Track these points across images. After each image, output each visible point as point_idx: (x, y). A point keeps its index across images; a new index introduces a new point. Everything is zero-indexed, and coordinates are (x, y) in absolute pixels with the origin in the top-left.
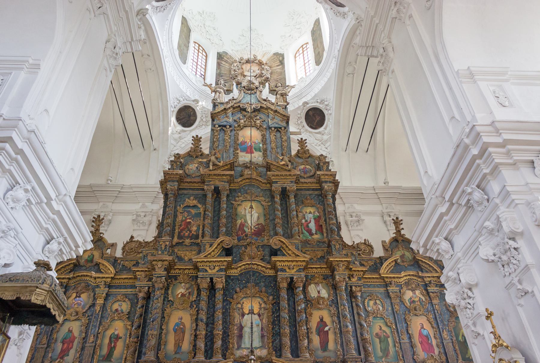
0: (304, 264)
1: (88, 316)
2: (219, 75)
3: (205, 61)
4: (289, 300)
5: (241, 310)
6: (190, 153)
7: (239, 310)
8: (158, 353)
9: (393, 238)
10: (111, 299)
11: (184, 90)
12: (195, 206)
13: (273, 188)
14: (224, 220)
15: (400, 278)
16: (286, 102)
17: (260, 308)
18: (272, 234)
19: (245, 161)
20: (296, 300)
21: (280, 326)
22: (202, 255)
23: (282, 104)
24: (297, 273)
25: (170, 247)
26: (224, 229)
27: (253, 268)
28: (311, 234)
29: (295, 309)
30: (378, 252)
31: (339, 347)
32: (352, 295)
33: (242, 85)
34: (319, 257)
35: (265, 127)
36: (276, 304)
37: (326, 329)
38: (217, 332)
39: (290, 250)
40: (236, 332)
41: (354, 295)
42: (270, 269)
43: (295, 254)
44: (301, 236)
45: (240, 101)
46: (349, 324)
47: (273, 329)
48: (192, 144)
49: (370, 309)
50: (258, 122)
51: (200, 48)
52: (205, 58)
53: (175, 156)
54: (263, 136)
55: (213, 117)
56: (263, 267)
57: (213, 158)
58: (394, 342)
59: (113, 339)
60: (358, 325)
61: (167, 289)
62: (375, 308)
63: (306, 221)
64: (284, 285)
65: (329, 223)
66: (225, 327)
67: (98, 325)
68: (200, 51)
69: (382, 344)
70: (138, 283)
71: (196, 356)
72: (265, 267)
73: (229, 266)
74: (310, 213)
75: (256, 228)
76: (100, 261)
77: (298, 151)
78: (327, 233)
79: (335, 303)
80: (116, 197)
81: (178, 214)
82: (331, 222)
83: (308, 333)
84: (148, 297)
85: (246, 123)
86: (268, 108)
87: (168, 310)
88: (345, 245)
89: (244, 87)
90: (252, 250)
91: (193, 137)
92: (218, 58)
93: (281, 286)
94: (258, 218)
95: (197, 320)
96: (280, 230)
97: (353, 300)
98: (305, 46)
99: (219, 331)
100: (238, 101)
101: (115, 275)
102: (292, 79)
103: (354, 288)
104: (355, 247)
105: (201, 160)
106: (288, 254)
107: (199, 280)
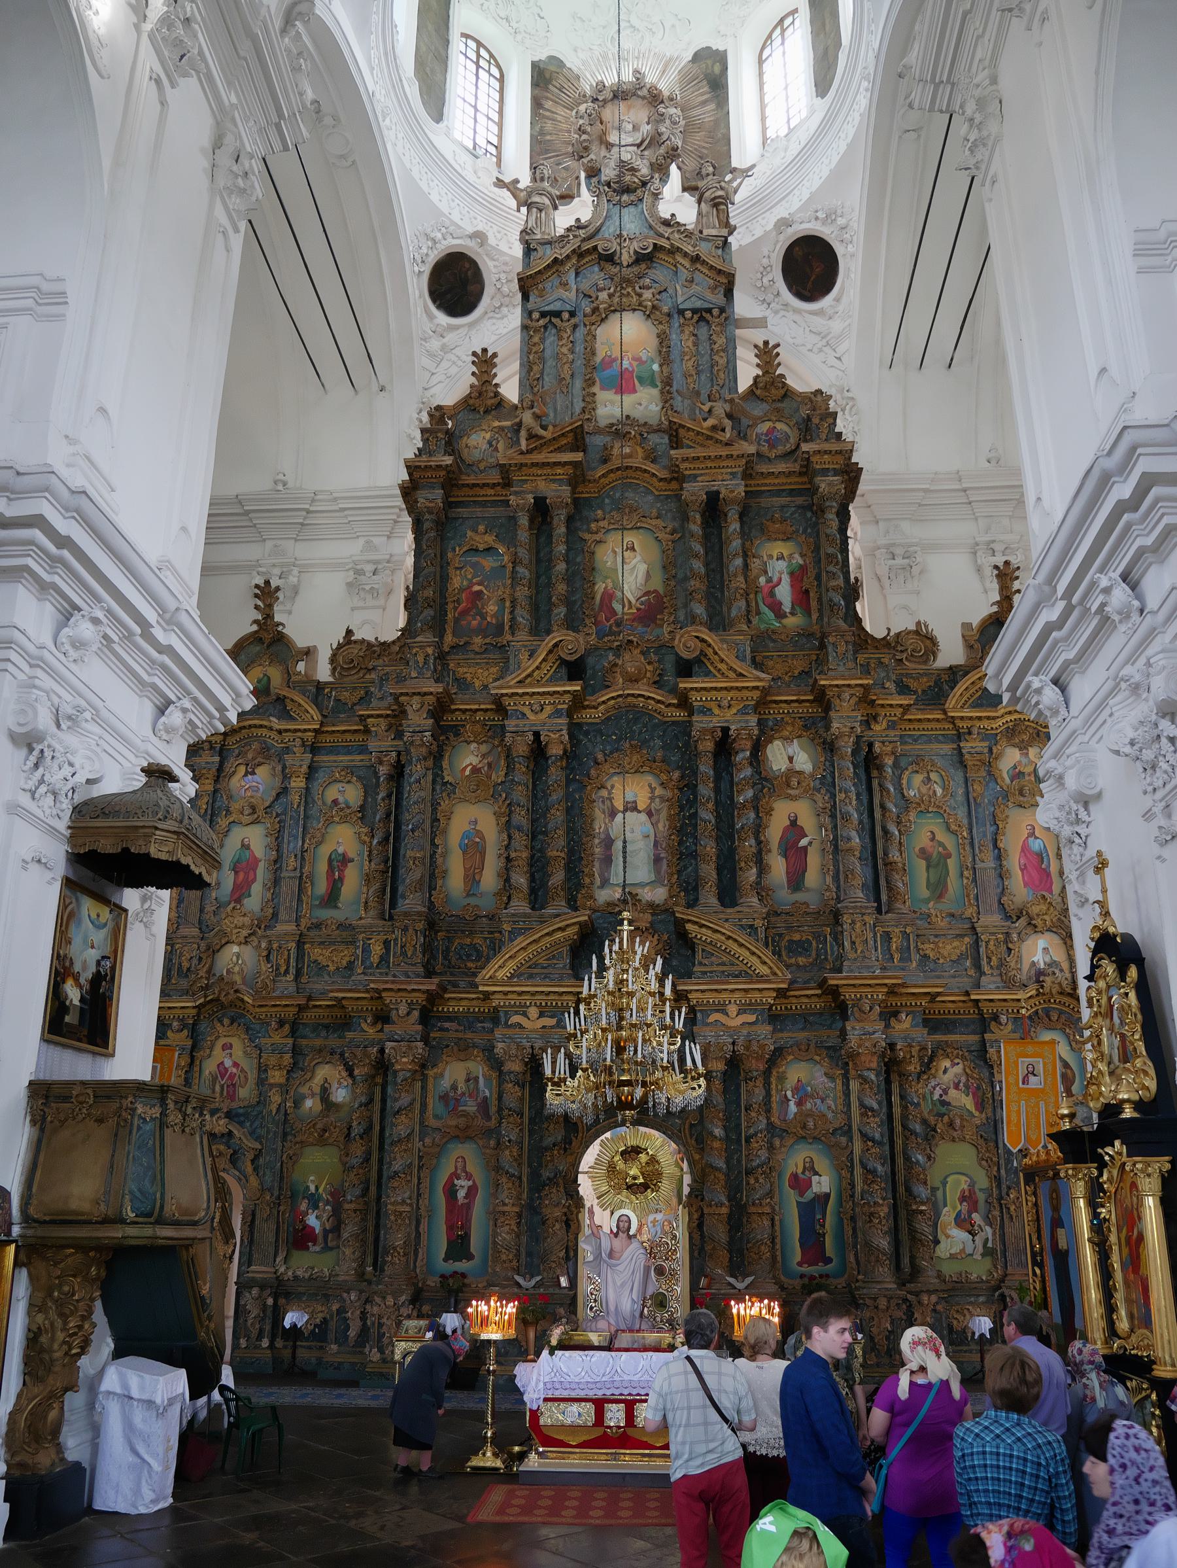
0: (756, 694)
1: (278, 815)
2: (540, 147)
3: (497, 96)
4: (718, 779)
5: (608, 803)
6: (471, 402)
7: (603, 802)
8: (431, 895)
9: (991, 616)
10: (321, 777)
11: (444, 207)
12: (489, 550)
13: (685, 495)
14: (561, 588)
15: (994, 718)
16: (727, 224)
17: (652, 799)
18: (682, 618)
19: (613, 416)
20: (736, 780)
21: (696, 838)
22: (512, 679)
23: (714, 232)
24: (738, 718)
25: (435, 659)
26: (561, 611)
27: (634, 706)
28: (780, 614)
29: (732, 798)
30: (951, 652)
31: (829, 880)
32: (869, 762)
33: (603, 178)
34: (796, 673)
35: (665, 309)
36: (687, 790)
37: (803, 842)
38: (555, 853)
39: (722, 661)
40: (597, 850)
41: (878, 762)
42: (678, 706)
43: (735, 671)
44: (755, 620)
45: (598, 230)
46: (854, 834)
47: (680, 843)
48: (473, 374)
49: (912, 794)
50: (647, 294)
51: (483, 52)
52: (497, 85)
53: (431, 415)
54: (663, 338)
55: (527, 285)
56: (659, 702)
57: (527, 418)
58: (962, 867)
59: (335, 863)
60: (879, 831)
61: (437, 756)
62: (924, 790)
63: (769, 580)
64: (708, 746)
65: (829, 585)
66: (572, 840)
67: (300, 835)
68: (482, 63)
69: (931, 870)
70: (373, 745)
71: (512, 904)
72: (663, 703)
73: (578, 703)
74: (781, 557)
75: (642, 604)
76: (284, 693)
77: (756, 378)
78: (820, 610)
79: (827, 783)
80: (302, 524)
81: (451, 571)
82: (833, 583)
83: (760, 852)
84: (398, 772)
85: (616, 300)
86: (674, 251)
87: (444, 805)
88: (863, 640)
89: (608, 184)
90: (631, 662)
91: (474, 354)
92: (535, 84)
93: (701, 747)
94: (648, 575)
95: (508, 827)
96: (699, 609)
97: (875, 773)
98: (790, 19)
99: (556, 850)
100: (591, 229)
101: (322, 724)
102: (745, 146)
103: (877, 748)
104: (891, 644)
105: (496, 424)
106: (719, 670)
107: (508, 739)
